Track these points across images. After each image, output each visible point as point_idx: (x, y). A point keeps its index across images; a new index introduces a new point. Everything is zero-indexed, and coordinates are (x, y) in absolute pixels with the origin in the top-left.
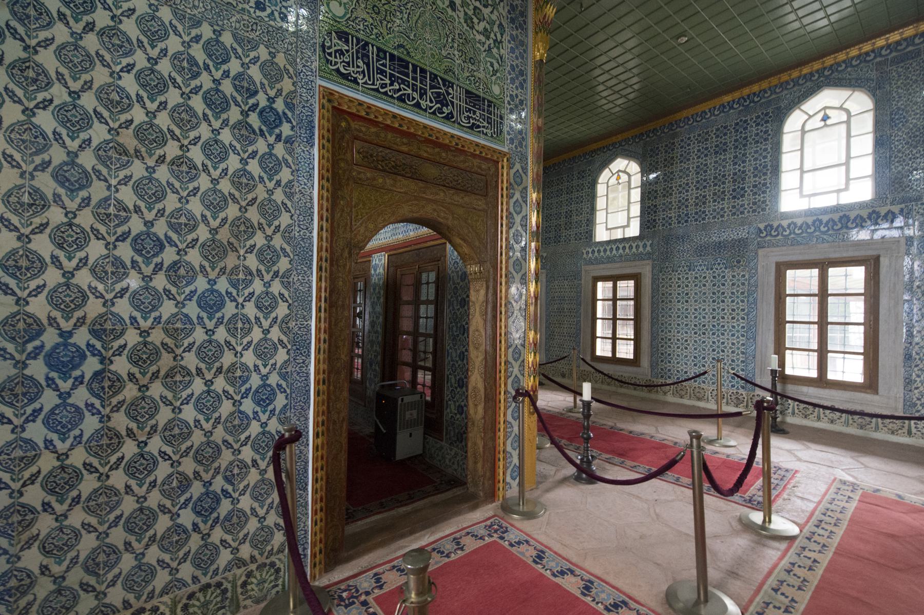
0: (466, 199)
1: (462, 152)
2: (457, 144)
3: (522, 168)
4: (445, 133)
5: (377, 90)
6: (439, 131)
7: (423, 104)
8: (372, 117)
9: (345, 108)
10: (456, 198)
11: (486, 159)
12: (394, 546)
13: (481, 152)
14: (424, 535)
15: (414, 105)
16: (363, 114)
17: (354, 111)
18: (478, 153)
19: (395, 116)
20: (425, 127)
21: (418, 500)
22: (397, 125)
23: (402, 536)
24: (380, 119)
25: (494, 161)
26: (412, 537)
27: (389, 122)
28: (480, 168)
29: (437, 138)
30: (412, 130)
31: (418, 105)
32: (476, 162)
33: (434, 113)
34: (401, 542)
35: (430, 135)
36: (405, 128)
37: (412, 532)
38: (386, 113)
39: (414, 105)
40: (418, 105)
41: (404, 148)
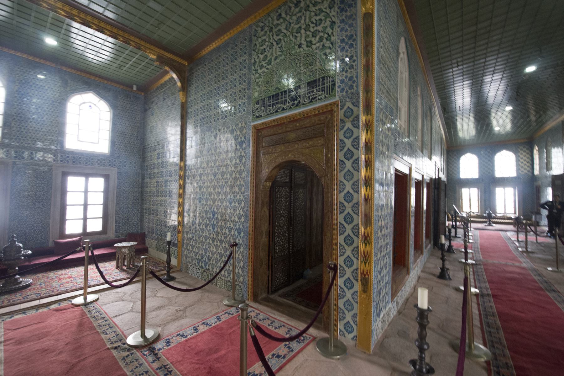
0: (310, 143)
1: (310, 117)
2: (304, 115)
3: (352, 103)
4: (296, 114)
5: (268, 114)
6: (292, 115)
7: (285, 107)
8: (268, 125)
9: (260, 128)
10: (304, 144)
11: (324, 113)
12: (273, 311)
13: (319, 111)
14: (285, 317)
15: (282, 110)
16: (265, 126)
17: (262, 127)
18: (317, 112)
19: (274, 121)
20: (286, 117)
21: (302, 305)
22: (276, 123)
23: (278, 310)
24: (270, 125)
25: (329, 111)
26: (281, 314)
27: (273, 124)
28: (320, 120)
29: (293, 118)
30: (282, 122)
31: (283, 109)
32: (316, 119)
33: (291, 108)
34: (277, 313)
35: (290, 119)
36: (279, 123)
37: (283, 313)
38: (271, 121)
39: (282, 110)
40: (283, 109)
41: (280, 131)
